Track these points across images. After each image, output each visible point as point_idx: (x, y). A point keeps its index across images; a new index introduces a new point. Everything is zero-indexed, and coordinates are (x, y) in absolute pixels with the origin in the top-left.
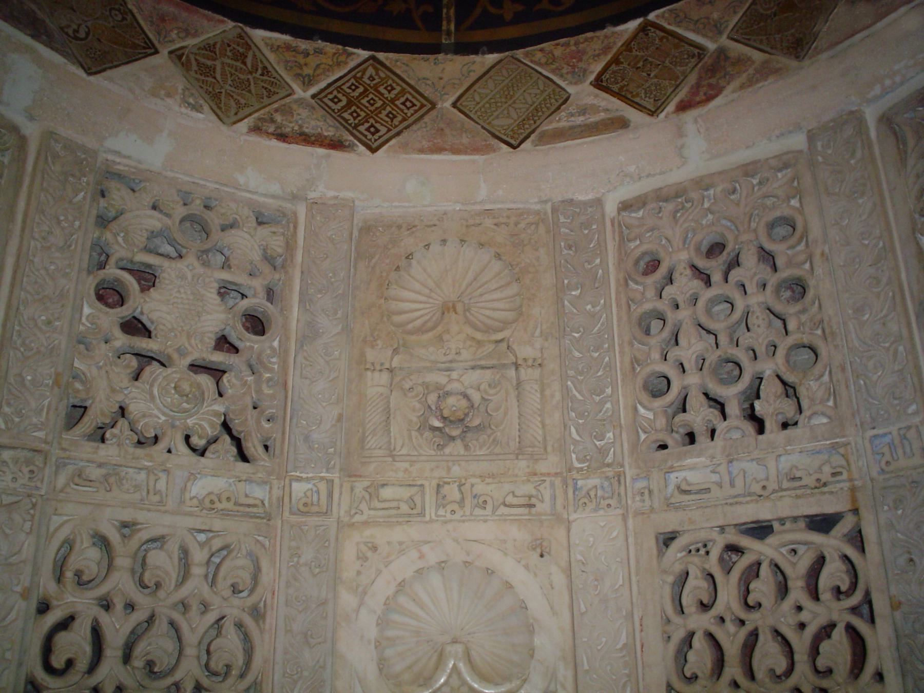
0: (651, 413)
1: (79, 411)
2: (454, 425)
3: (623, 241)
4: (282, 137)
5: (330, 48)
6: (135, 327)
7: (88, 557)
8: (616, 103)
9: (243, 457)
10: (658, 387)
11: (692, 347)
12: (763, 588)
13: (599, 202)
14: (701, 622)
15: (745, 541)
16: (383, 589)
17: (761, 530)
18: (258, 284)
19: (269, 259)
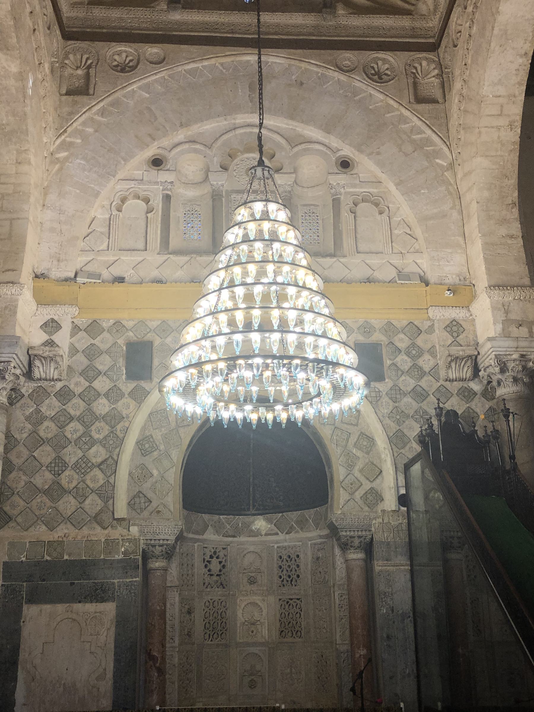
1: (204, 584)
2: (252, 581)
3: (277, 553)
4: (226, 537)
5: (232, 517)
6: (209, 570)
7: (207, 604)
8: (277, 530)
9: (224, 588)
10: (280, 577)
11: (285, 572)
12: (291, 606)
13: (273, 546)
14: (284, 611)
15: (289, 601)
16: (243, 606)
17: (291, 599)
18: (224, 560)
19: (225, 556)
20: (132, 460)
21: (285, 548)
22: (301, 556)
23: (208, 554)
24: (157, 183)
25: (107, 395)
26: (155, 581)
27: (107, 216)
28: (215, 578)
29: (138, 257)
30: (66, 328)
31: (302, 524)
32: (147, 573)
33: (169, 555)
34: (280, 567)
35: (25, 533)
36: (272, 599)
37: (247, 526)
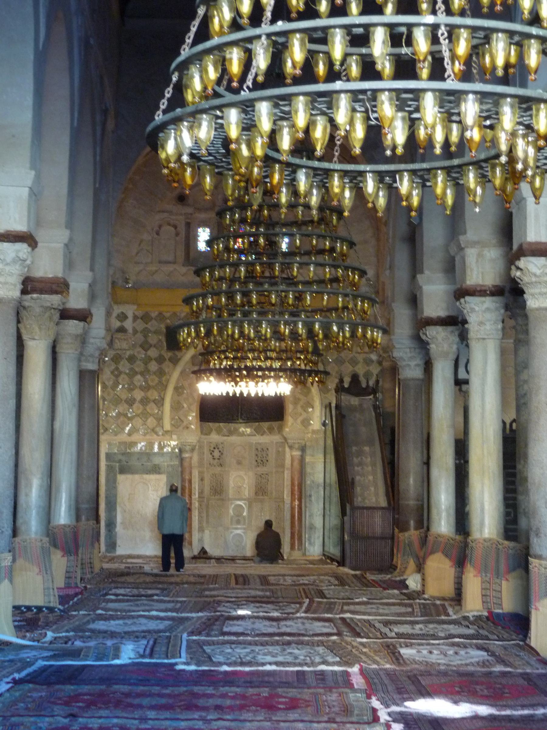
0: (256, 463)
2: (239, 463)
20: (172, 398)
21: (260, 444)
22: (270, 449)
23: (213, 446)
24: (181, 214)
25: (156, 359)
26: (186, 464)
27: (150, 238)
28: (216, 461)
29: (171, 268)
30: (130, 319)
31: (271, 430)
32: (182, 460)
33: (193, 450)
34: (257, 455)
35: (116, 437)
36: (251, 474)
37: (236, 430)
